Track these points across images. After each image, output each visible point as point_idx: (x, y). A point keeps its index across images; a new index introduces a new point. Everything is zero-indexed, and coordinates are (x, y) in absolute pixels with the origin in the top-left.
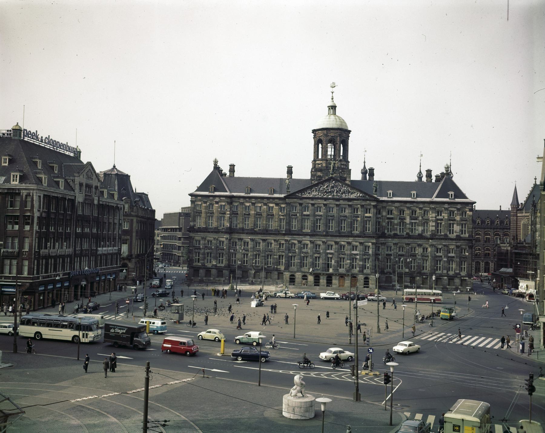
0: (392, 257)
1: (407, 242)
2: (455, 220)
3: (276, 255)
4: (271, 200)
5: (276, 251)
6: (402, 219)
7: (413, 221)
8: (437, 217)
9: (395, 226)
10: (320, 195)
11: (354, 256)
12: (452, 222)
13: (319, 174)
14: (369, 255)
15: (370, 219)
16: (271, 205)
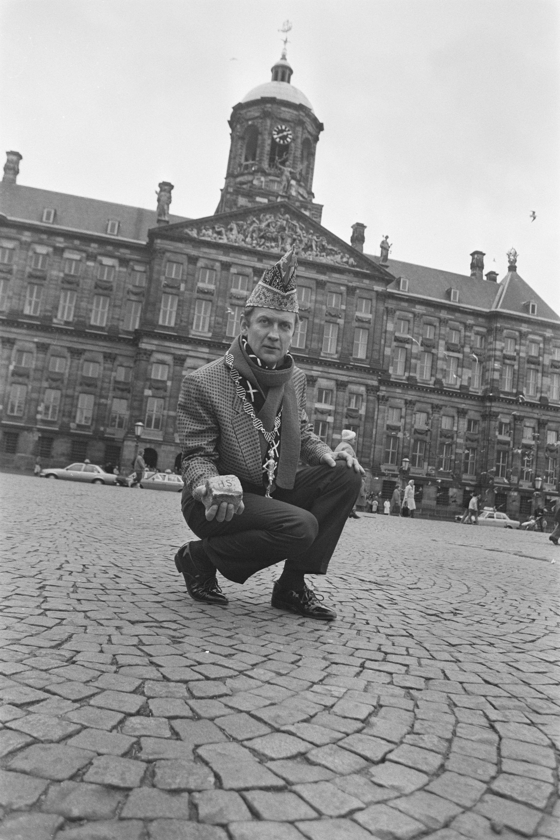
0: (400, 435)
1: (436, 402)
2: (538, 363)
3: (106, 398)
4: (110, 248)
5: (106, 385)
6: (428, 346)
7: (451, 354)
8: (504, 352)
9: (413, 361)
10: (250, 243)
11: (320, 417)
12: (533, 366)
13: (242, 201)
14: (360, 417)
15: (367, 325)
16: (107, 261)
